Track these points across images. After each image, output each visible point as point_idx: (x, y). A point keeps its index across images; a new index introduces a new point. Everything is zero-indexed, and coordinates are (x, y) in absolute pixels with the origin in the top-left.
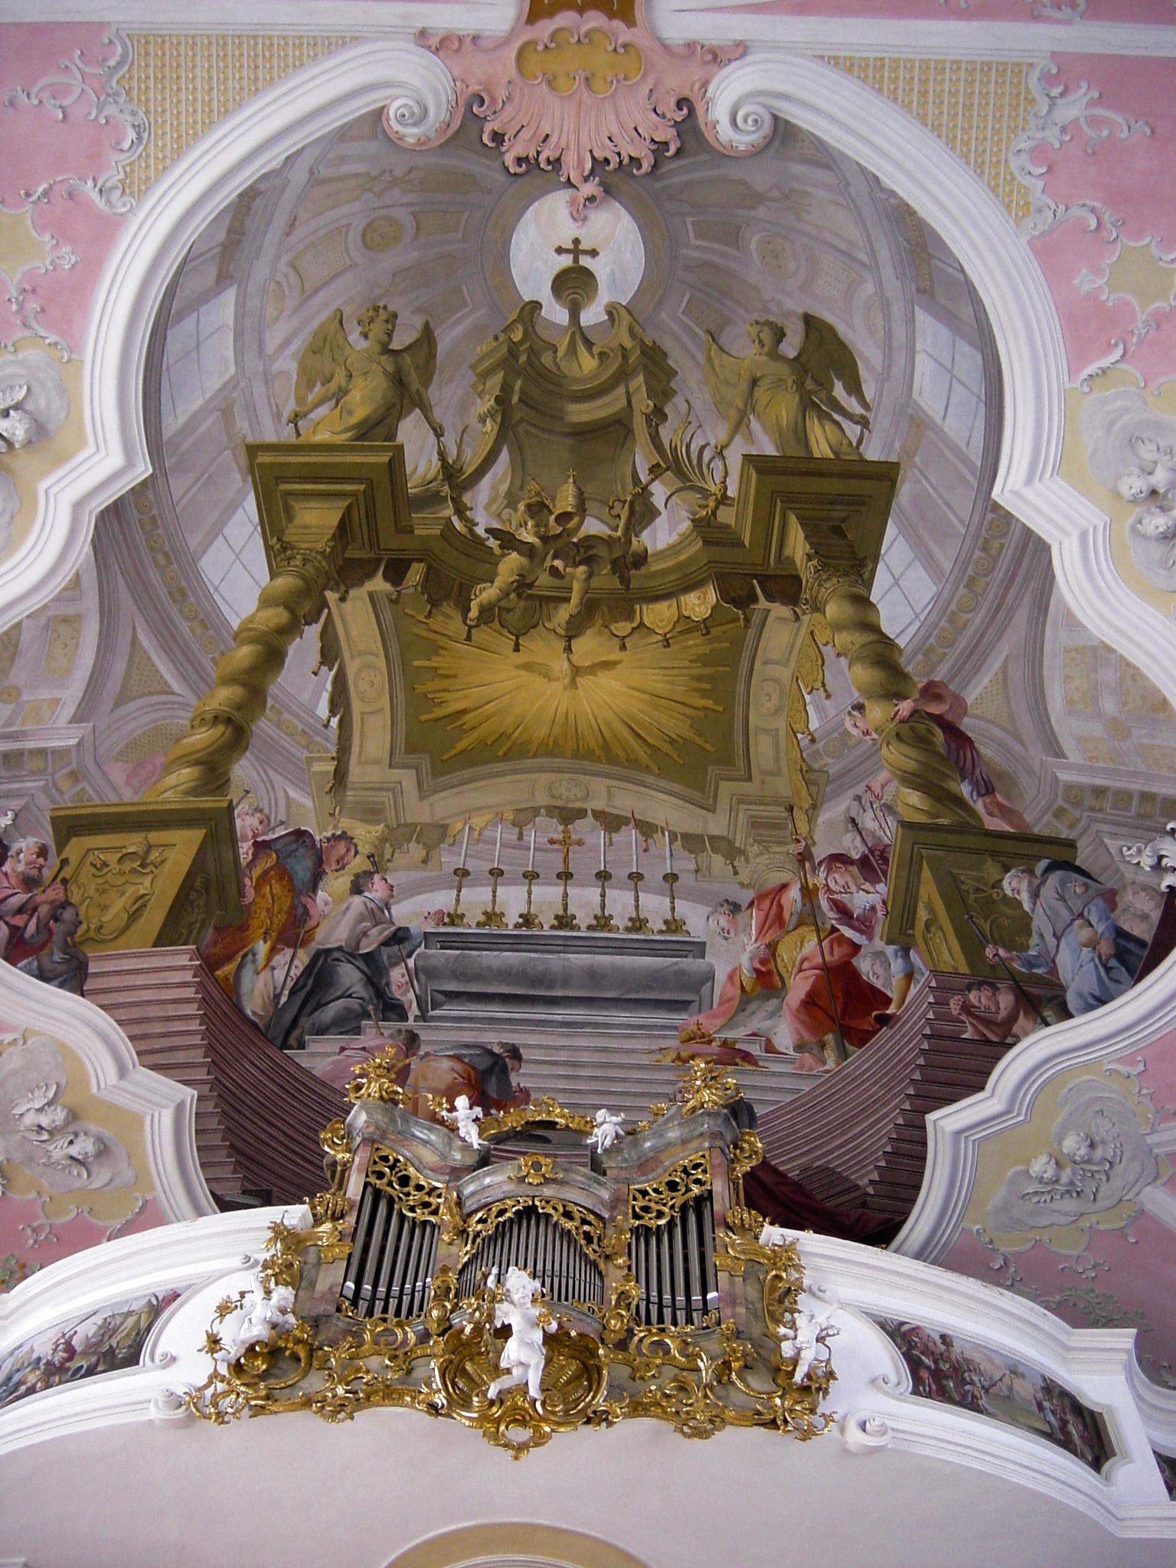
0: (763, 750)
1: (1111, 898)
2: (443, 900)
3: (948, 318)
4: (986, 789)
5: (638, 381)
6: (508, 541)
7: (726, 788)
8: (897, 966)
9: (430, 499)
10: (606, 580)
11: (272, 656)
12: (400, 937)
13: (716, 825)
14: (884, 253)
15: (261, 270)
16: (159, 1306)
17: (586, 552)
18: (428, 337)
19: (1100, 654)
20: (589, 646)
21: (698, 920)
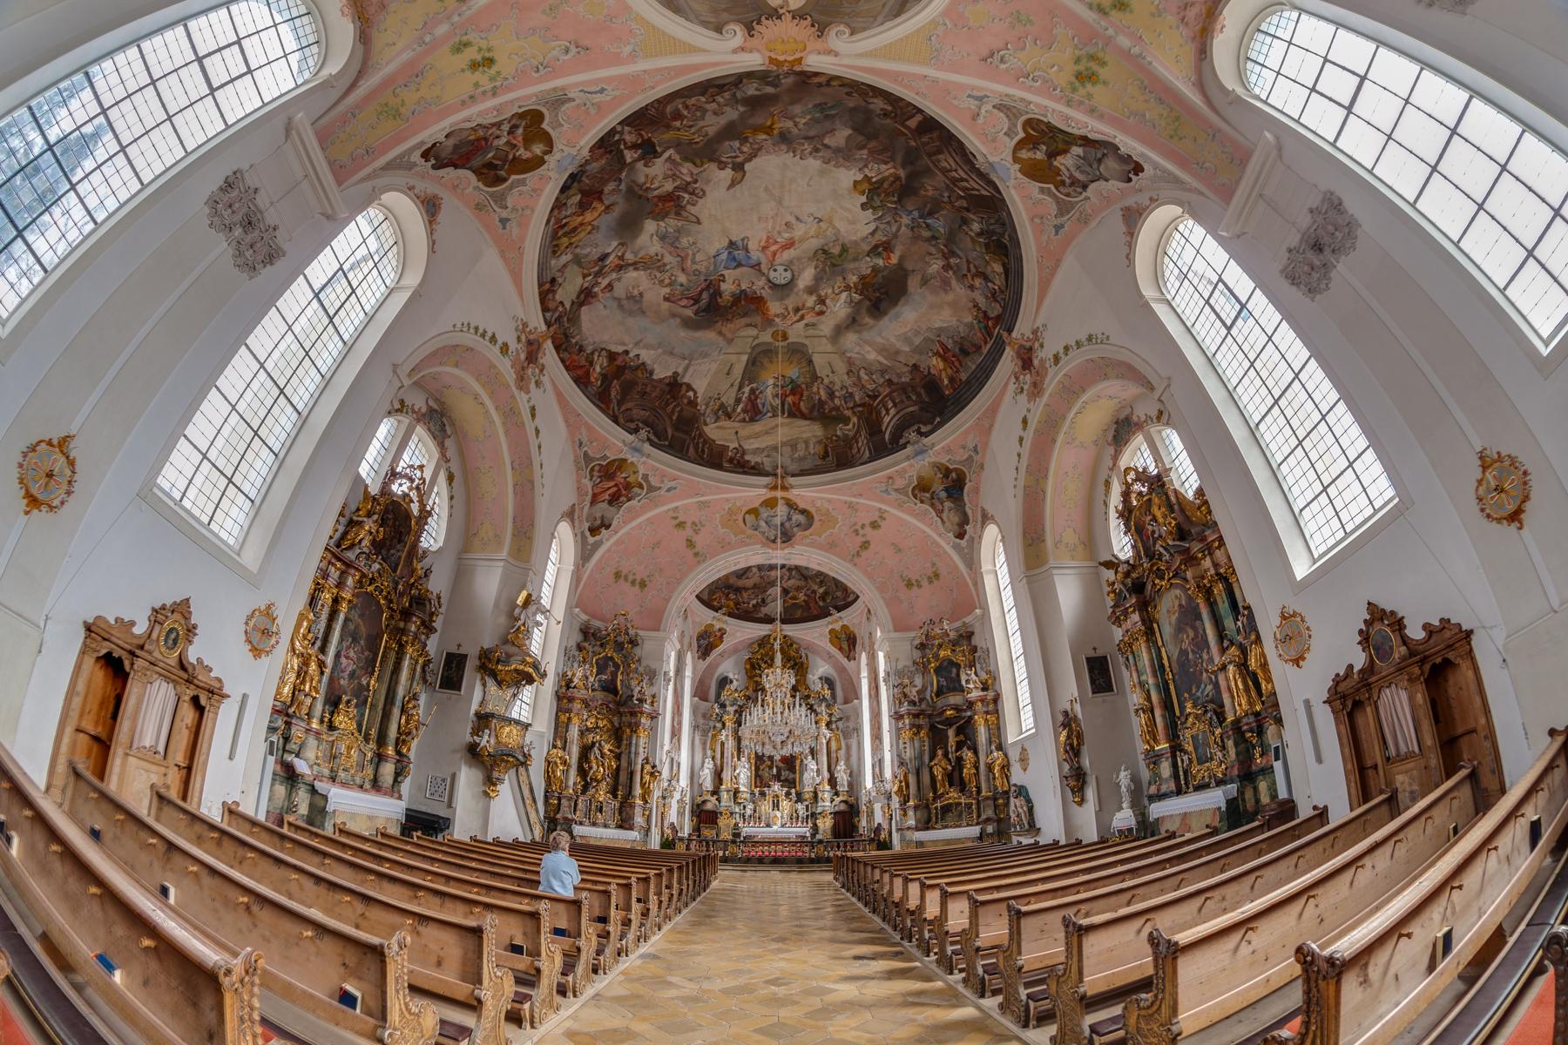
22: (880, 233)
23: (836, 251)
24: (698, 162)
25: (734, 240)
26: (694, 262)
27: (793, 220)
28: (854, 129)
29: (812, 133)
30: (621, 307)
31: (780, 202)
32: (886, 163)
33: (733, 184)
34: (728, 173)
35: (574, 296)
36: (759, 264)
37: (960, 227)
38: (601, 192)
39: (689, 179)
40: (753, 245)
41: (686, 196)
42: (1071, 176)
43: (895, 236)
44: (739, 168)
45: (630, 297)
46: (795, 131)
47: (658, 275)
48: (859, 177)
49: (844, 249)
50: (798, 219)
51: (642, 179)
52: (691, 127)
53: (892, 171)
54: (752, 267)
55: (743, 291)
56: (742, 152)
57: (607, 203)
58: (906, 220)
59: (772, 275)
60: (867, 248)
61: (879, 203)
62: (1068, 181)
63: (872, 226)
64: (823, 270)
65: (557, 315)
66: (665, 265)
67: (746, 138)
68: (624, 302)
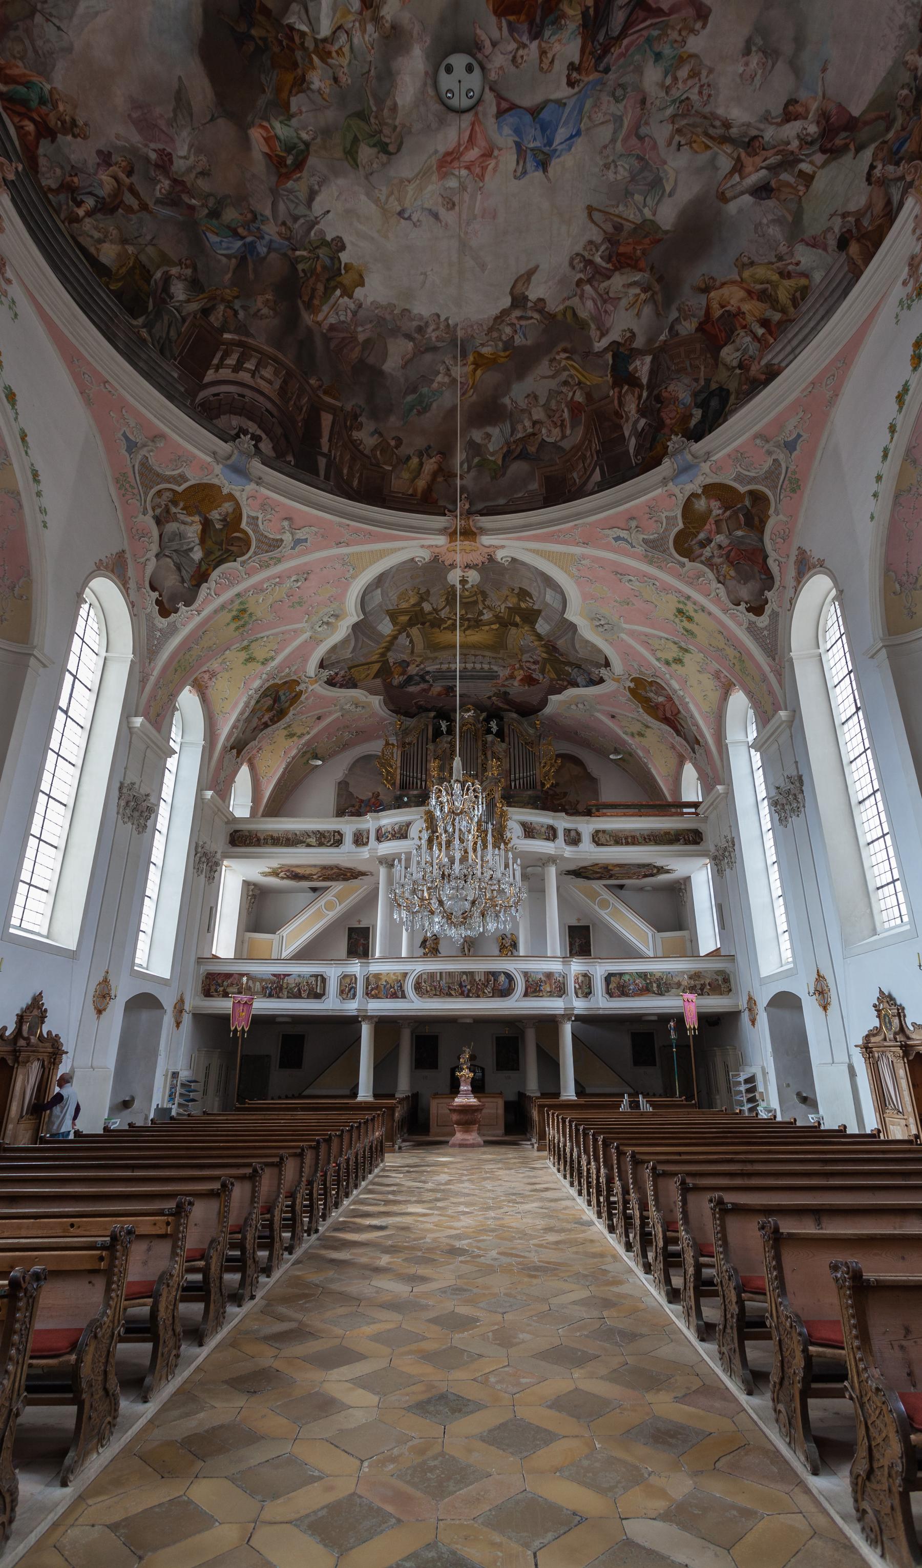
0: (510, 646)
1: (589, 674)
2: (438, 666)
3: (554, 590)
4: (562, 655)
5: (479, 596)
6: (449, 619)
7: (502, 651)
8: (541, 677)
9: (430, 613)
10: (472, 623)
11: (395, 637)
12: (428, 672)
13: (500, 656)
14: (539, 579)
15: (387, 585)
16: (408, 824)
17: (468, 620)
18: (428, 592)
19: (587, 642)
20: (467, 632)
21: (495, 668)
22: (303, 195)
23: (366, 152)
24: (569, 315)
25: (539, 174)
26: (618, 120)
27: (442, 212)
28: (381, 373)
29: (428, 357)
30: (800, 41)
31: (464, 246)
32: (332, 328)
33: (530, 274)
34: (535, 292)
35: (851, 154)
36: (500, 113)
37: (195, 269)
38: (700, 328)
39: (587, 288)
40: (508, 159)
41: (598, 260)
42: (176, 519)
43: (274, 192)
44: (519, 301)
45: (770, 53)
46: (449, 361)
47: (694, 96)
48: (359, 293)
49: (351, 154)
50: (436, 216)
51: (647, 310)
52: (566, 383)
53: (320, 317)
54: (513, 107)
55: (536, 35)
56: (512, 325)
57: (703, 300)
58: (271, 230)
59: (474, 80)
60: (312, 161)
61: (321, 252)
62: (173, 510)
63: (318, 207)
64: (380, 102)
65: (891, 168)
66: (673, 118)
67: (505, 350)
68: (787, 48)
